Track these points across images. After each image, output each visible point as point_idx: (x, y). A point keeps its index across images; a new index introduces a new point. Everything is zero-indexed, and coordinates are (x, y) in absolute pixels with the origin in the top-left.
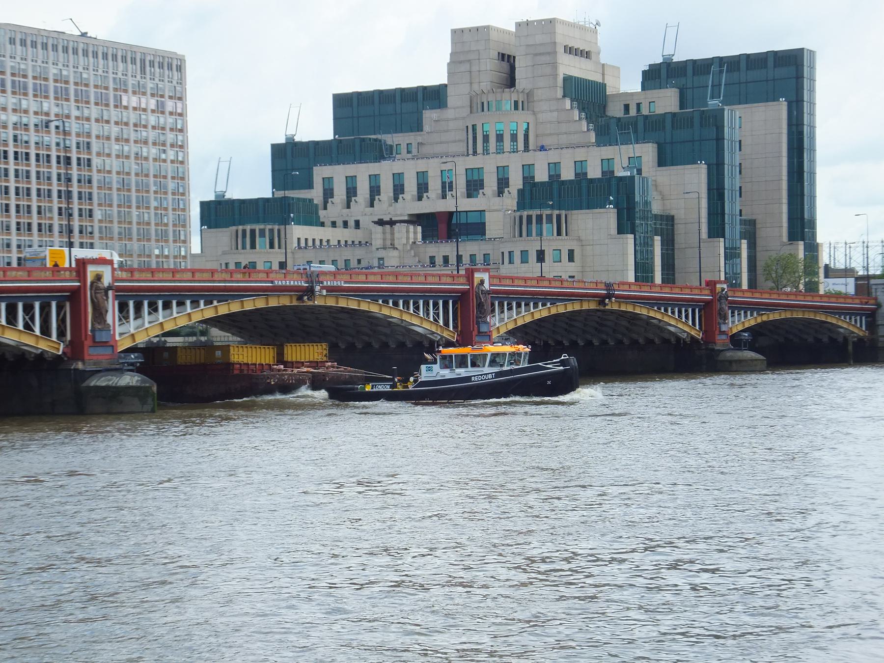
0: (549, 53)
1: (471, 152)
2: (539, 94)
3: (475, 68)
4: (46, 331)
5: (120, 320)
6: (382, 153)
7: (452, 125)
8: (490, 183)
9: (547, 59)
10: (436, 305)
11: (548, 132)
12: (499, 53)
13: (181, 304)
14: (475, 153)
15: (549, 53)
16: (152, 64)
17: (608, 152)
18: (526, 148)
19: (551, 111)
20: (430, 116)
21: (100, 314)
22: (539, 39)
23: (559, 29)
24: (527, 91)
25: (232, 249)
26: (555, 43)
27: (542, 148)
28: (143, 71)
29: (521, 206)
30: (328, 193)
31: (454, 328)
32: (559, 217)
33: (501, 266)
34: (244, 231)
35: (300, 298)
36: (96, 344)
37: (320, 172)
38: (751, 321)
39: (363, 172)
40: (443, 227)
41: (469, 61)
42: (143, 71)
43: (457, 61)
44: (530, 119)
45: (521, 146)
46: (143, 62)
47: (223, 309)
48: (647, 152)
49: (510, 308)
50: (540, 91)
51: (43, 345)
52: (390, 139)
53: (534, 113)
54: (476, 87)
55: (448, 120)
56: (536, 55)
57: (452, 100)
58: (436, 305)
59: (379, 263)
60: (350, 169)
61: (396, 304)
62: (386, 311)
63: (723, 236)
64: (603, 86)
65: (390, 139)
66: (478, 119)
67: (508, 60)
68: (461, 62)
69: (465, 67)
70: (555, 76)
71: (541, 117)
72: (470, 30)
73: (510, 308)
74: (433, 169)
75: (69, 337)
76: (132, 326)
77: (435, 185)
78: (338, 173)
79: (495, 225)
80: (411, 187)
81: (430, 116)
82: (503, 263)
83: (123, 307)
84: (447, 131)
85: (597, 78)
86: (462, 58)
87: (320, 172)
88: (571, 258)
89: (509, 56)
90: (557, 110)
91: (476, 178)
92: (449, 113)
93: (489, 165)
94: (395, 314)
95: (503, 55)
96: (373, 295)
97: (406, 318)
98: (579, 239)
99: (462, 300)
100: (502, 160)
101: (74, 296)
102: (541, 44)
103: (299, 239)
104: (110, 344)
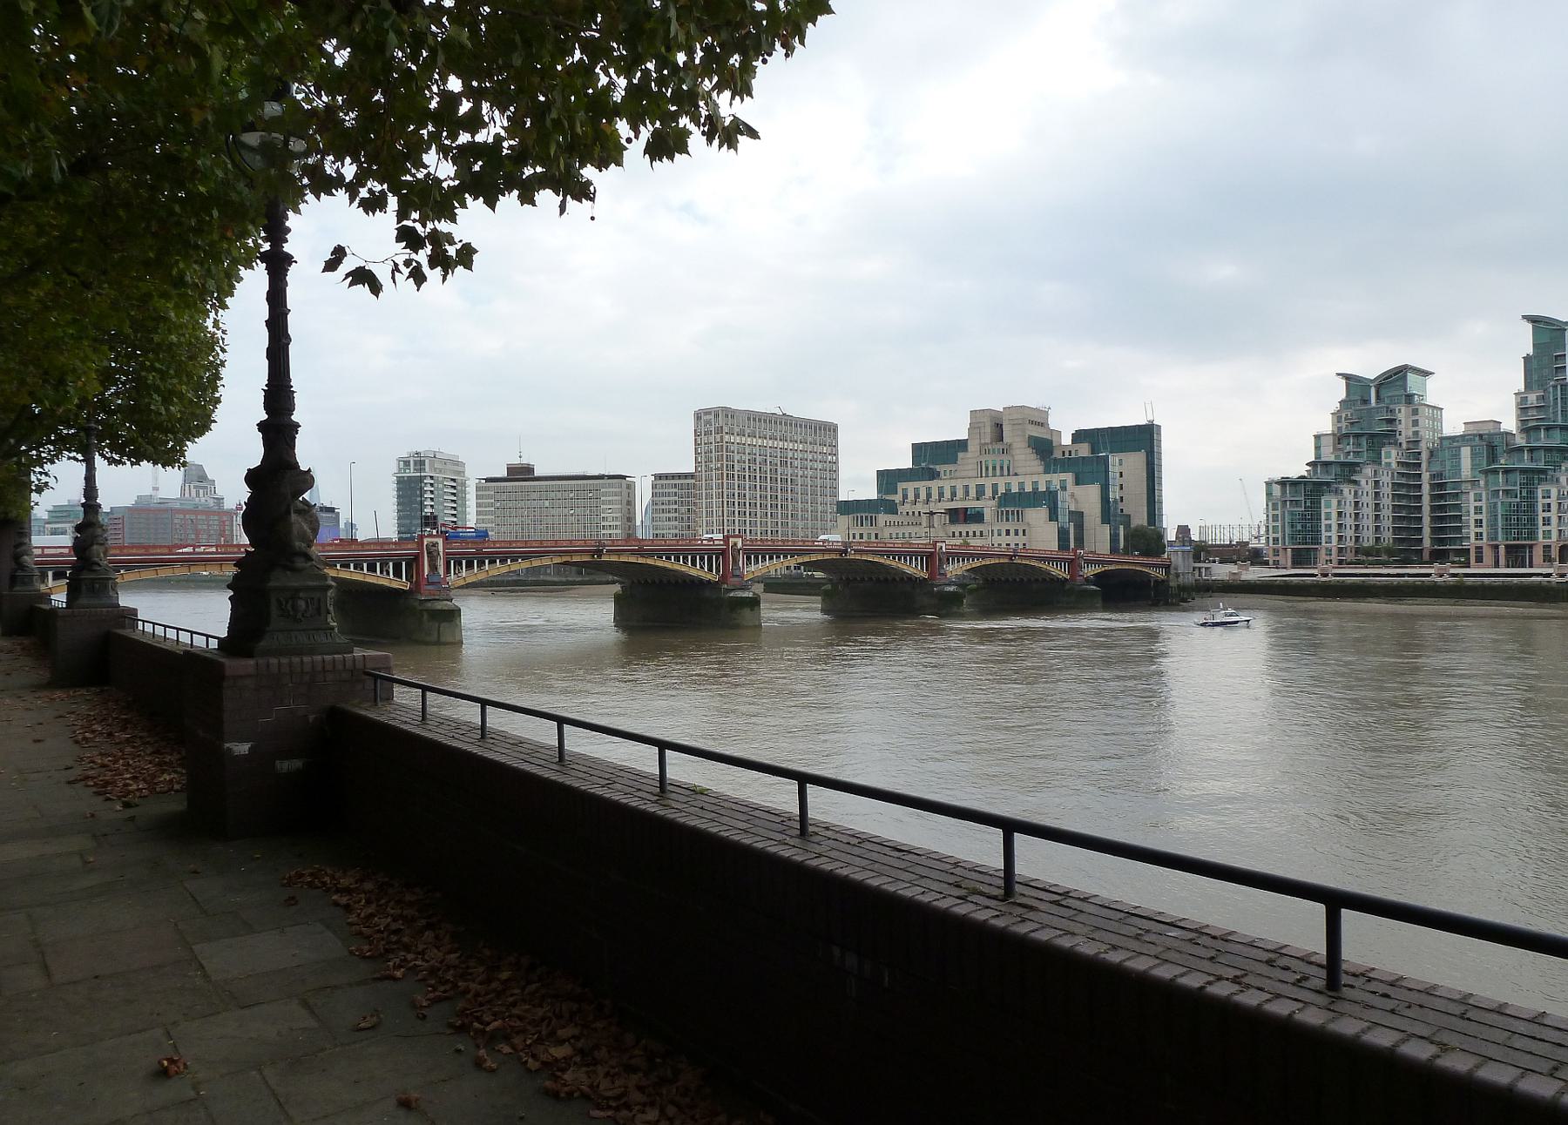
2: (1015, 445)
3: (982, 431)
4: (710, 570)
5: (747, 564)
6: (934, 475)
7: (970, 461)
9: (1020, 427)
10: (916, 559)
13: (778, 557)
14: (981, 477)
17: (1048, 477)
18: (1009, 475)
20: (960, 455)
21: (735, 561)
27: (1016, 474)
29: (1000, 506)
30: (905, 496)
31: (406, 580)
34: (857, 517)
35: (841, 555)
36: (734, 576)
37: (901, 486)
38: (1099, 569)
39: (922, 485)
40: (961, 517)
41: (979, 428)
43: (973, 428)
45: (1006, 473)
47: (807, 559)
48: (1069, 477)
49: (958, 562)
51: (709, 577)
52: (938, 468)
57: (970, 448)
58: (916, 559)
61: (894, 558)
62: (888, 562)
64: (1051, 442)
65: (938, 468)
67: (999, 427)
73: (958, 562)
75: (414, 579)
76: (753, 568)
77: (960, 494)
78: (910, 487)
79: (988, 515)
80: (947, 495)
81: (960, 455)
83: (749, 558)
85: (1048, 437)
86: (977, 426)
87: (901, 486)
88: (1024, 535)
92: (969, 455)
93: (988, 483)
94: (893, 564)
96: (888, 554)
97: (900, 565)
98: (1028, 524)
99: (930, 556)
101: (723, 553)
104: (741, 576)
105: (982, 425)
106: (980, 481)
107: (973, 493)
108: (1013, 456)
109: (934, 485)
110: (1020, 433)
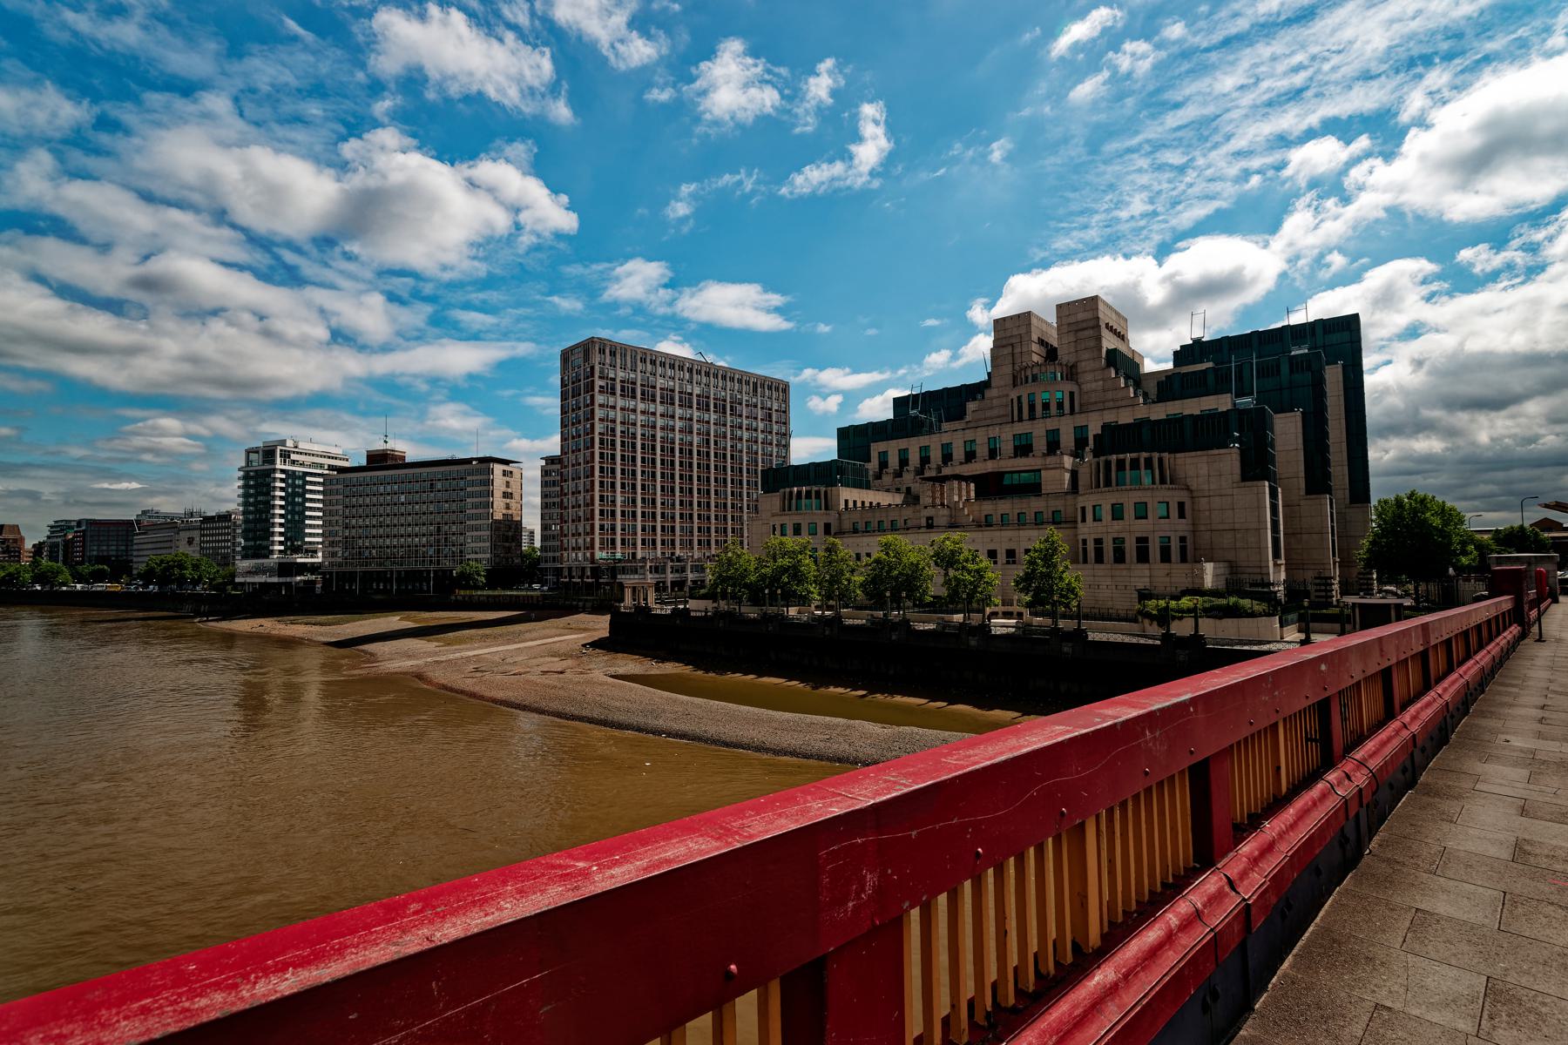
1: (1016, 418)
2: (1082, 366)
3: (1017, 350)
8: (1040, 445)
9: (1090, 332)
11: (1093, 400)
15: (1093, 328)
16: (763, 386)
19: (1096, 381)
20: (971, 406)
22: (1081, 316)
24: (1070, 365)
25: (784, 510)
26: (1098, 318)
28: (755, 390)
29: (1096, 454)
30: (883, 464)
32: (1161, 460)
33: (1080, 525)
37: (876, 448)
39: (913, 445)
41: (1012, 345)
42: (755, 390)
44: (1075, 389)
46: (755, 384)
50: (1083, 363)
53: (1079, 385)
54: (1017, 368)
55: (992, 399)
56: (1077, 331)
59: (927, 522)
60: (902, 443)
63: (1329, 490)
66: (1023, 391)
68: (1003, 347)
69: (1008, 350)
70: (1100, 348)
71: (1083, 386)
74: (981, 438)
78: (892, 448)
82: (1084, 520)
84: (992, 408)
86: (1004, 342)
87: (876, 448)
88: (1182, 515)
89: (1047, 343)
90: (1103, 380)
91: (1024, 442)
95: (1043, 341)
98: (1188, 489)
100: (1051, 424)
102: (1083, 321)
103: (846, 501)
105: (1013, 341)
106: (1020, 428)
107: (1007, 447)
108: (1079, 385)
109: (934, 443)
110: (1092, 343)
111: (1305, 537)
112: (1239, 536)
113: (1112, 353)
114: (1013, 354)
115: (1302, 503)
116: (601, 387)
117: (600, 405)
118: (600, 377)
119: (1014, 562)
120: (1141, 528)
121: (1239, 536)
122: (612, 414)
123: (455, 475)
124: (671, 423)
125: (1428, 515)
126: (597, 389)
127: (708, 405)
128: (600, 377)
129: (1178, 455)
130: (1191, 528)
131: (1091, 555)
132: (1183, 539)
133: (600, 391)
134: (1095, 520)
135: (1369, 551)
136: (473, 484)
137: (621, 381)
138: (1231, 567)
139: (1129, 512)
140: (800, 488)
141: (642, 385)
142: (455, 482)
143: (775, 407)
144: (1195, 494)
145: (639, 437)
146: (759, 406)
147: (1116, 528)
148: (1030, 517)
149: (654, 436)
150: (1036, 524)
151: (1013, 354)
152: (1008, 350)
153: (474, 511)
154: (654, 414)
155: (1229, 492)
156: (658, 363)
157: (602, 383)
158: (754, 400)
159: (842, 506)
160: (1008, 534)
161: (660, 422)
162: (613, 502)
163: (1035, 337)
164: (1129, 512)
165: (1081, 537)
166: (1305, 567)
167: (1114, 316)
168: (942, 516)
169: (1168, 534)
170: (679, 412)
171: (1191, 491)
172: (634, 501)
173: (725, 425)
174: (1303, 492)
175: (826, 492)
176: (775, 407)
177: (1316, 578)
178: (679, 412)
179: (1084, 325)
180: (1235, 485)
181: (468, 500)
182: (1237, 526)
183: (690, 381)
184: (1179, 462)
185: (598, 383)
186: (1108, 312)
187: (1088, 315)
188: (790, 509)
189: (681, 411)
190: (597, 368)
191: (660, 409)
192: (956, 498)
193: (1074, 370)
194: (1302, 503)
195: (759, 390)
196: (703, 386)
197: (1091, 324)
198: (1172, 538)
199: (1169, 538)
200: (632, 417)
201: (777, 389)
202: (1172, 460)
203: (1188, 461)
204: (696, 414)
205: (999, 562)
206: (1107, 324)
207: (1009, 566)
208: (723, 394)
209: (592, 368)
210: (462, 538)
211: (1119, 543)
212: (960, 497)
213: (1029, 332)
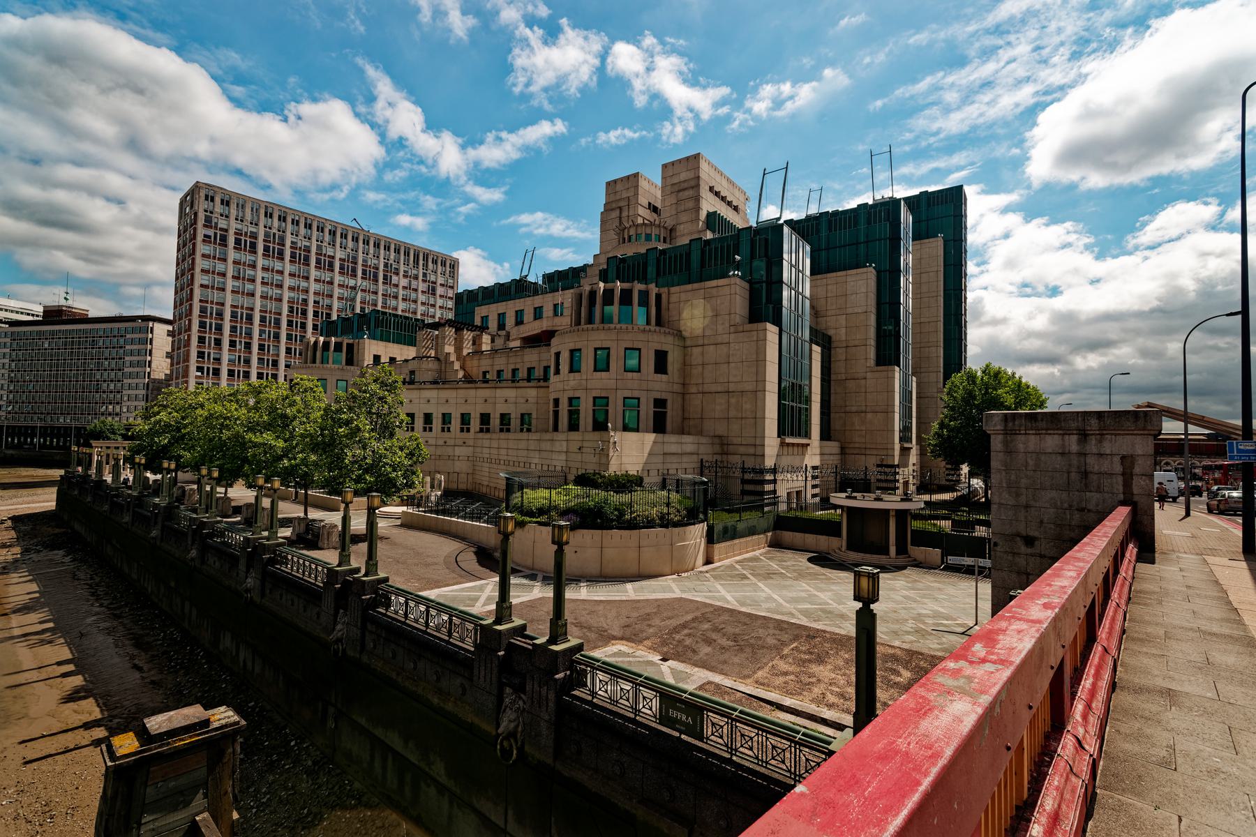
0: (692, 187)
3: (625, 214)
12: (650, 204)
15: (692, 187)
22: (684, 176)
23: (704, 166)
50: (682, 226)
56: (679, 191)
68: (612, 210)
69: (616, 214)
70: (697, 209)
72: (622, 179)
82: (557, 372)
86: (614, 205)
87: (480, 312)
102: (685, 181)
105: (622, 204)
110: (691, 204)
111: (869, 416)
112: (733, 400)
113: (712, 216)
114: (620, 218)
115: (869, 375)
116: (205, 236)
117: (203, 256)
118: (205, 226)
119: (488, 430)
120: (601, 382)
121: (733, 400)
122: (220, 267)
123: (116, 333)
124: (304, 284)
125: (1000, 391)
126: (200, 238)
127: (354, 270)
128: (205, 226)
129: (673, 289)
130: (677, 388)
131: (586, 418)
132: (660, 403)
133: (204, 241)
134: (571, 371)
135: (938, 435)
136: (132, 342)
137: (236, 233)
138: (722, 444)
139: (587, 362)
140: (328, 339)
141: (264, 241)
142: (115, 340)
143: (440, 280)
144: (688, 343)
145: (311, 303)
146: (421, 277)
147: (572, 383)
148: (522, 374)
149: (305, 301)
150: (513, 381)
151: (620, 218)
152: (616, 214)
153: (131, 370)
154: (281, 273)
155: (725, 338)
156: (289, 220)
157: (211, 232)
158: (414, 272)
159: (368, 360)
160: (485, 393)
161: (313, 287)
162: (218, 360)
163: (643, 201)
164: (587, 362)
165: (552, 396)
166: (868, 452)
167: (724, 183)
168: (428, 370)
169: (636, 394)
170: (314, 274)
171: (684, 339)
172: (247, 362)
173: (376, 293)
174: (872, 362)
175: (350, 347)
176: (440, 280)
177: (878, 466)
178: (314, 274)
179: (686, 185)
180: (732, 329)
181: (127, 358)
182: (732, 387)
183: (333, 244)
184: (674, 298)
185: (201, 232)
186: (712, 173)
187: (690, 175)
188: (314, 361)
189: (318, 273)
190: (201, 216)
191: (288, 268)
192: (449, 349)
193: (673, 234)
194: (869, 375)
195: (421, 262)
196: (349, 250)
197: (693, 183)
198: (643, 400)
199: (639, 399)
200: (250, 272)
201: (444, 264)
202: (664, 297)
203: (683, 296)
204: (338, 279)
205: (472, 430)
206: (711, 189)
207: (480, 435)
208: (376, 262)
209: (196, 214)
210: (119, 396)
211: (601, 403)
212: (459, 349)
213: (636, 194)
